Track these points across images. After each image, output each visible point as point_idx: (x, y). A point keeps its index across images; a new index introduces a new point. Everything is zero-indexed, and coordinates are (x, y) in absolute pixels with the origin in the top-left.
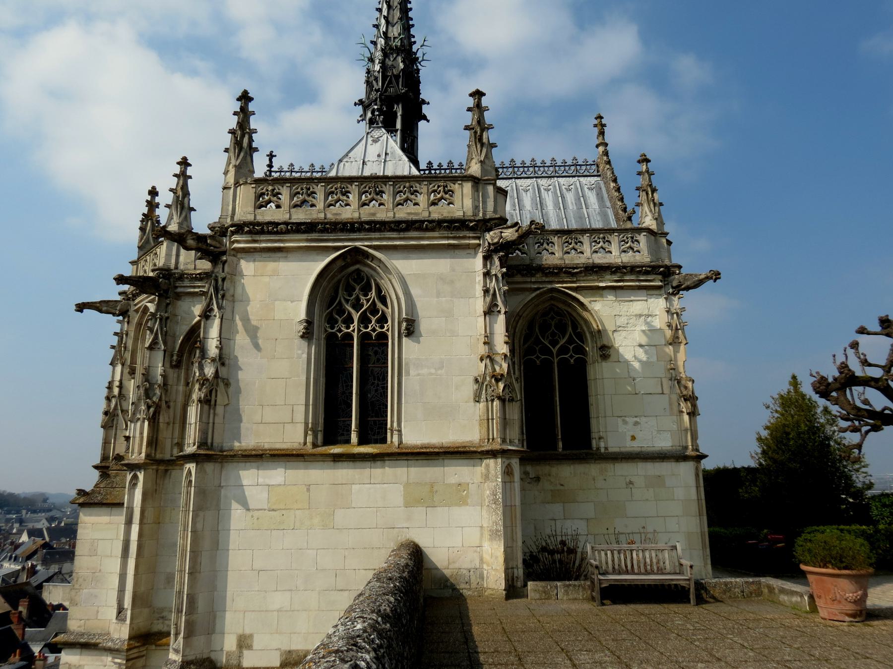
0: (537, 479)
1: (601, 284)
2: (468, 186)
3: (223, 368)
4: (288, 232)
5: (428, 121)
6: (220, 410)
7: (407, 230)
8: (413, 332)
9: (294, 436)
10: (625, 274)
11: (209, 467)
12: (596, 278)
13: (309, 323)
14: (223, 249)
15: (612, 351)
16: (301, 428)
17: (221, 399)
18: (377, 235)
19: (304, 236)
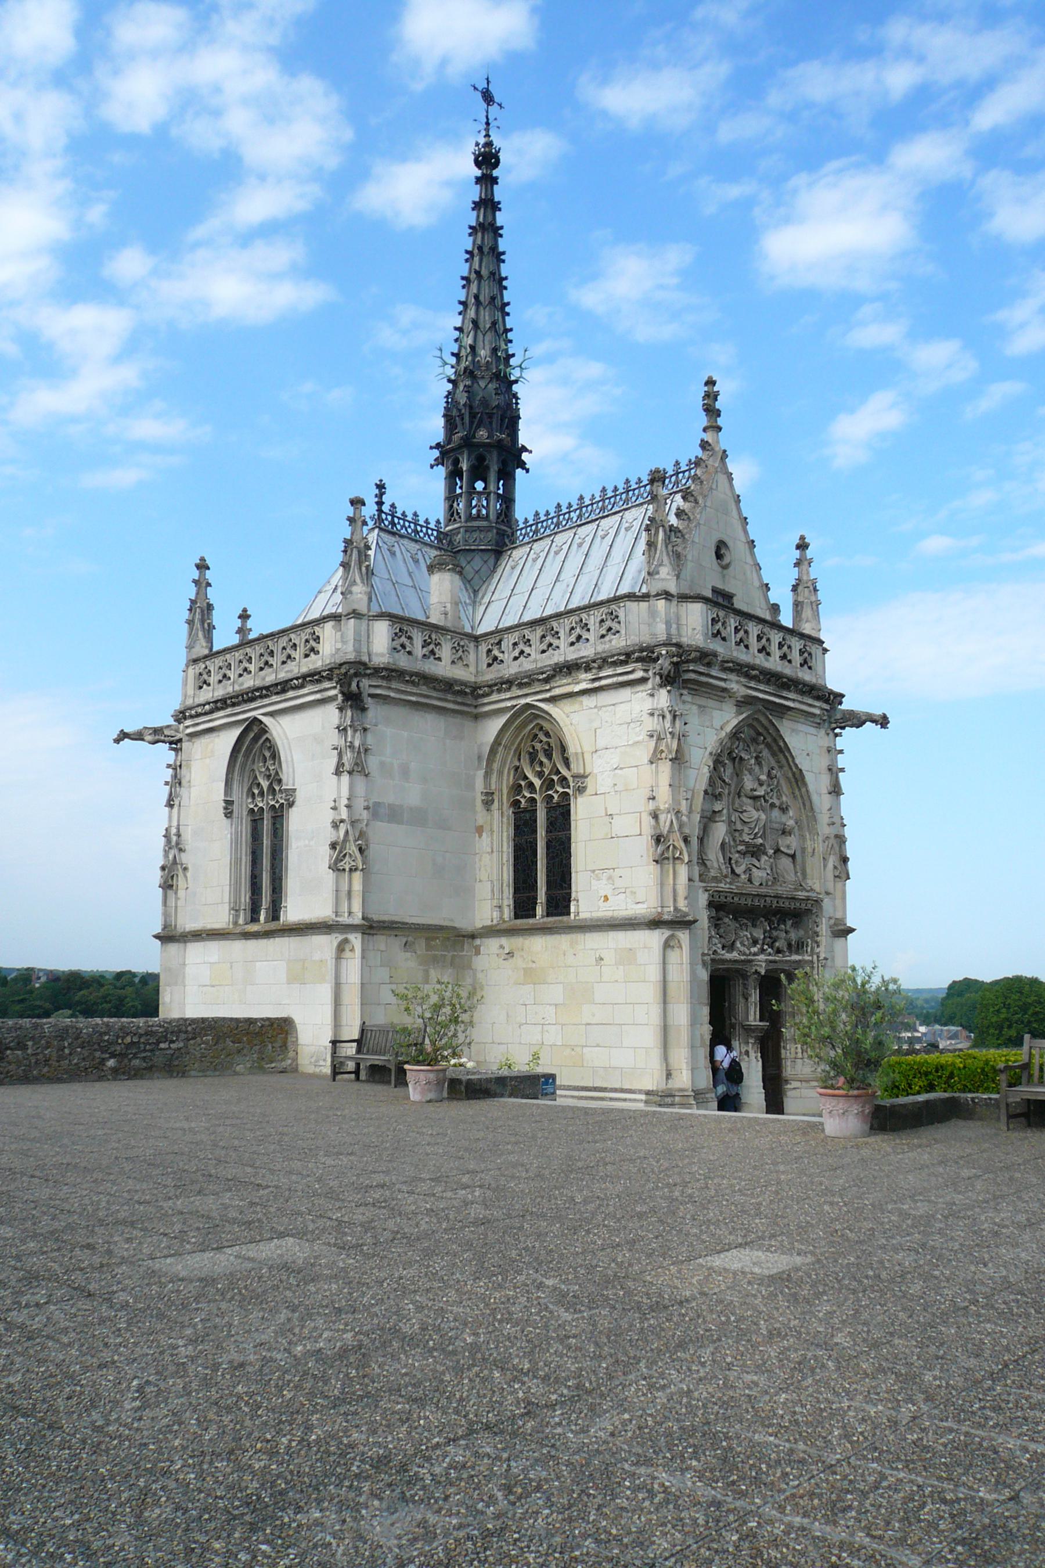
0: (511, 954)
1: (577, 688)
2: (329, 626)
3: (182, 854)
4: (211, 712)
5: (531, 452)
6: (181, 893)
7: (284, 691)
8: (293, 802)
9: (220, 918)
10: (600, 668)
11: (173, 948)
12: (570, 680)
13: (229, 803)
14: (179, 736)
15: (589, 782)
16: (227, 907)
17: (181, 882)
18: (266, 701)
19: (221, 713)
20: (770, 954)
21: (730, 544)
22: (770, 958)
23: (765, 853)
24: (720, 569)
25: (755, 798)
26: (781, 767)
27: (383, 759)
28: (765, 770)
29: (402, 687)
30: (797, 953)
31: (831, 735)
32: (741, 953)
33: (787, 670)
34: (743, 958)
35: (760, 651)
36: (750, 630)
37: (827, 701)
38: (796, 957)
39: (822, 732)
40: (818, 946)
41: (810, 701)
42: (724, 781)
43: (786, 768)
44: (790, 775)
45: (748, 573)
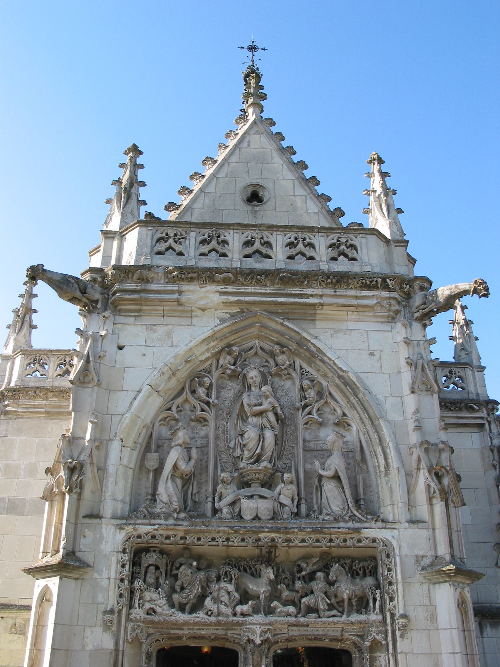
20: (289, 615)
21: (269, 185)
22: (289, 619)
23: (283, 481)
24: (249, 208)
25: (260, 414)
26: (325, 376)
27: (9, 462)
28: (297, 382)
29: (31, 402)
30: (359, 612)
31: (417, 326)
32: (210, 613)
33: (301, 265)
34: (213, 619)
35: (247, 256)
36: (229, 238)
37: (386, 287)
38: (355, 617)
39: (399, 325)
40: (391, 599)
41: (353, 293)
42: (208, 403)
43: (330, 375)
44: (338, 381)
45: (299, 203)
